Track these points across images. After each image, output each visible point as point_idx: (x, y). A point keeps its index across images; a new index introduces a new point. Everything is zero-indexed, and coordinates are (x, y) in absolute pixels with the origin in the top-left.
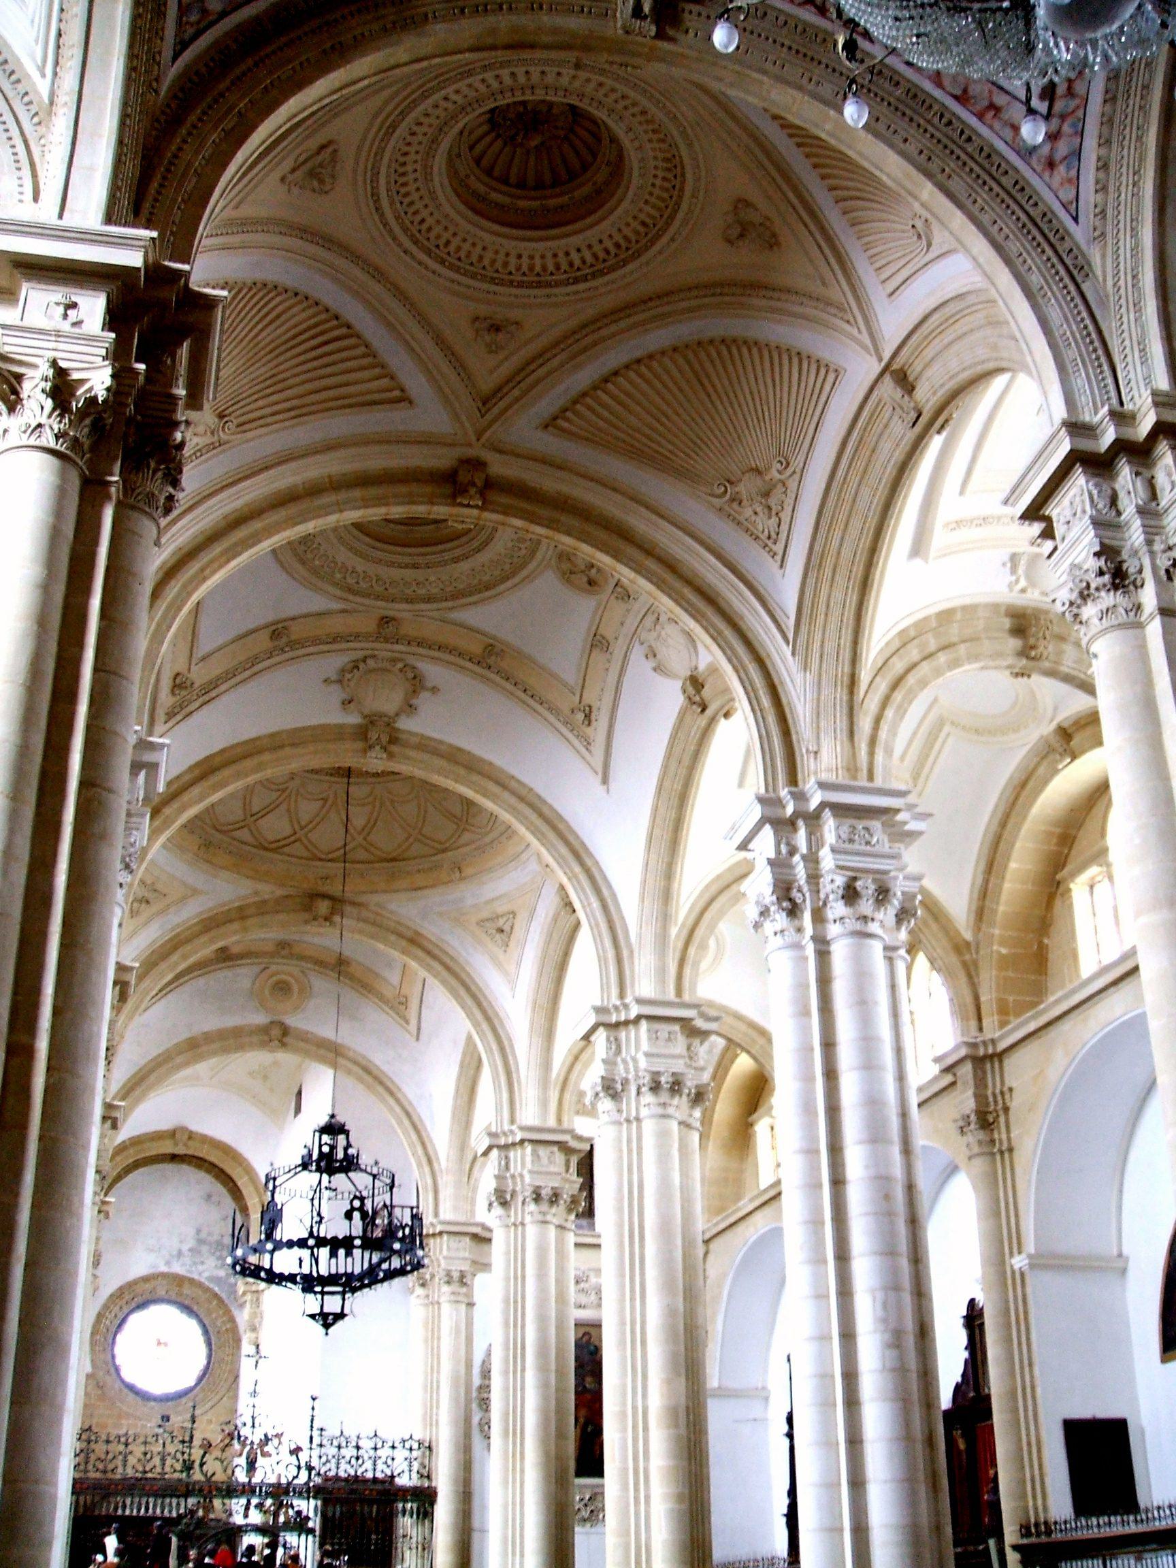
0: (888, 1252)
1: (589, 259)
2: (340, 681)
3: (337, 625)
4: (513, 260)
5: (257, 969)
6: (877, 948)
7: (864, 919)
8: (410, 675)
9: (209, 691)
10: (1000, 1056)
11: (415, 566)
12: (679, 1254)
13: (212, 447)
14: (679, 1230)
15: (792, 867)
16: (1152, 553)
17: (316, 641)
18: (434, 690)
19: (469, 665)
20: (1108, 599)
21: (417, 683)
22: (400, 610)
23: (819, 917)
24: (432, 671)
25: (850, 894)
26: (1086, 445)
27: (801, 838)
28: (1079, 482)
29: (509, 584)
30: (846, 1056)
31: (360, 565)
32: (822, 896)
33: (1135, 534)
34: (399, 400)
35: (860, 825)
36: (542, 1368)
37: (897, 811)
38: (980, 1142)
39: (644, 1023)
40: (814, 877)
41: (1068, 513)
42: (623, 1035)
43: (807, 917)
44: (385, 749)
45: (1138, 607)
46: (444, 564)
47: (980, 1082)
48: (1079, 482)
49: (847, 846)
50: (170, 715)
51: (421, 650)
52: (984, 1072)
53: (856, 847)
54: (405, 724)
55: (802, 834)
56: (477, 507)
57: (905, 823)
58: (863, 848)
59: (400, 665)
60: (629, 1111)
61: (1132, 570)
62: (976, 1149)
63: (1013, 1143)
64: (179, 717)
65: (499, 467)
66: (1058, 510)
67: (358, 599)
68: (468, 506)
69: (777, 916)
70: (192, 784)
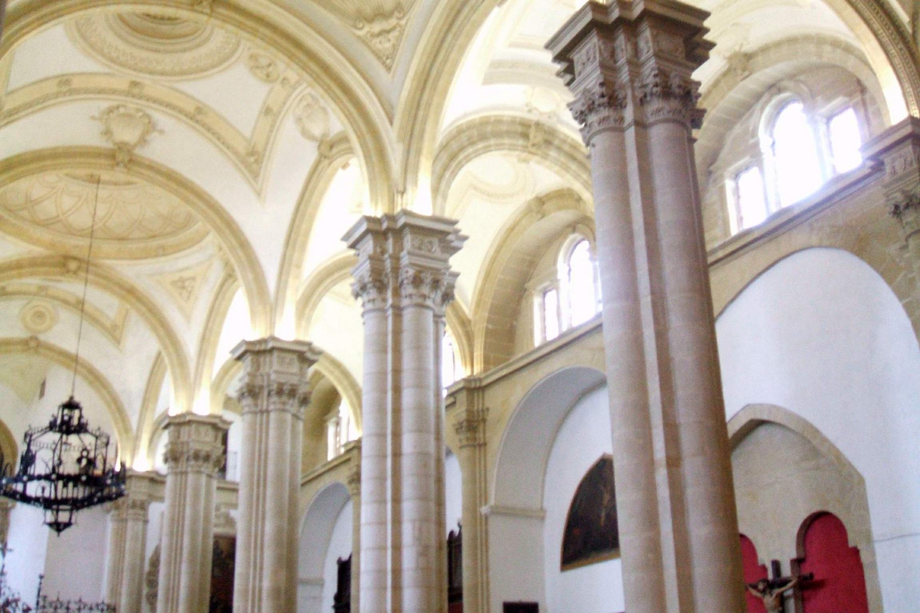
0: (423, 498)
2: (100, 119)
3: (104, 83)
5: (25, 302)
6: (429, 315)
7: (424, 297)
8: (146, 121)
10: (483, 389)
11: (156, 51)
12: (286, 494)
14: (288, 479)
15: (383, 261)
16: (633, 89)
17: (87, 91)
18: (162, 132)
19: (184, 118)
20: (605, 112)
21: (151, 126)
23: (397, 293)
24: (161, 118)
25: (417, 281)
26: (600, 17)
27: (390, 244)
28: (594, 42)
29: (216, 70)
30: (407, 379)
31: (122, 46)
32: (400, 280)
33: (624, 76)
35: (427, 240)
36: (192, 561)
37: (448, 233)
38: (468, 439)
39: (276, 354)
40: (396, 269)
41: (584, 58)
42: (262, 359)
43: (389, 294)
44: (125, 166)
45: (622, 119)
46: (176, 52)
47: (471, 402)
48: (594, 42)
49: (417, 251)
51: (154, 105)
52: (474, 398)
53: (423, 252)
54: (138, 151)
55: (390, 241)
56: (207, 14)
57: (452, 242)
58: (427, 253)
59: (140, 114)
60: (262, 406)
61: (620, 96)
62: (465, 442)
63: (487, 440)
66: (578, 57)
67: (117, 67)
68: (202, 13)
69: (371, 291)
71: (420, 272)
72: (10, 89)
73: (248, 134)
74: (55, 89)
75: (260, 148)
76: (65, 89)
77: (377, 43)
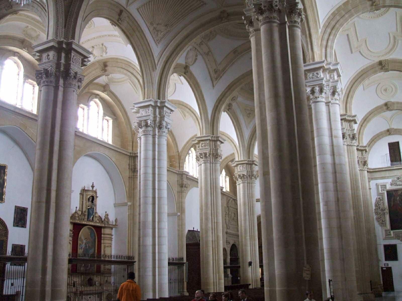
7: (316, 98)
9: (224, 70)
13: (167, 33)
34: (202, 5)
50: (216, 79)
56: (227, 22)
64: (219, 79)
65: (230, 10)
68: (225, 22)
70: (227, 92)
71: (313, 88)
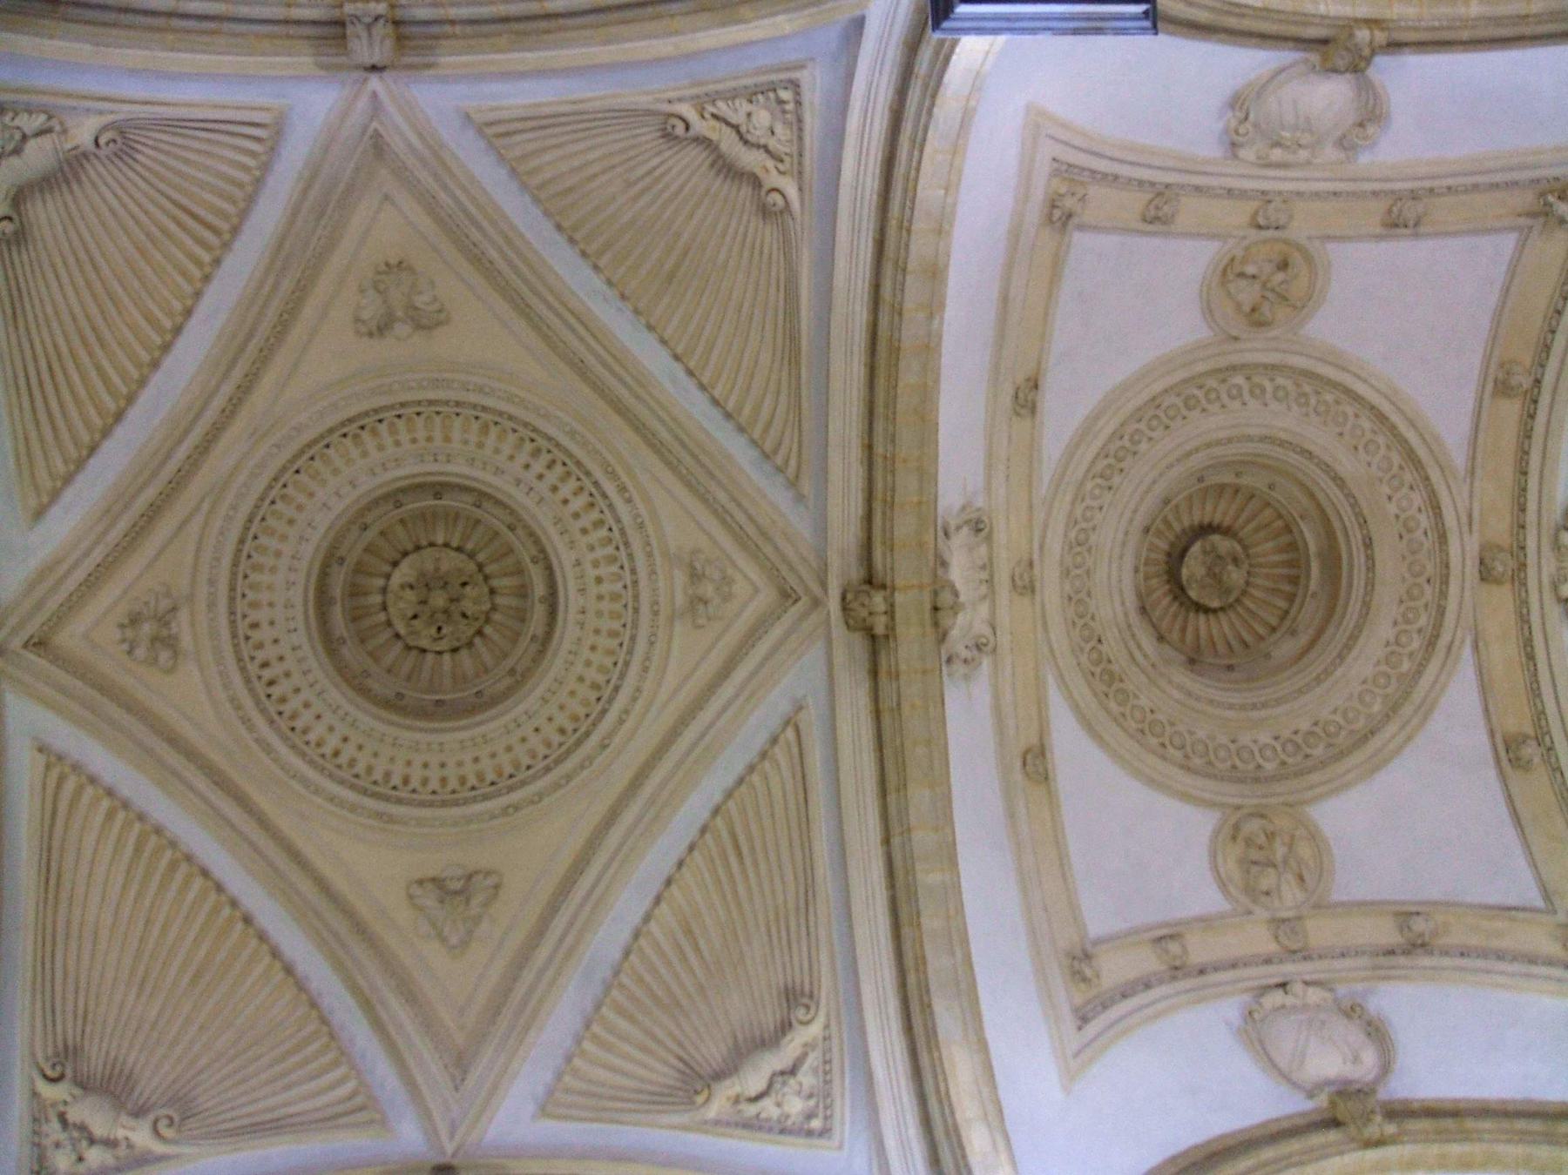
1: (572, 484)
3: (1503, 654)
4: (605, 588)
22: (1463, 552)
29: (1360, 388)
31: (1382, 630)
72: (1539, 903)
73: (1509, 242)
74: (1540, 777)
75: (1527, 199)
76: (1530, 751)
77: (782, 139)
